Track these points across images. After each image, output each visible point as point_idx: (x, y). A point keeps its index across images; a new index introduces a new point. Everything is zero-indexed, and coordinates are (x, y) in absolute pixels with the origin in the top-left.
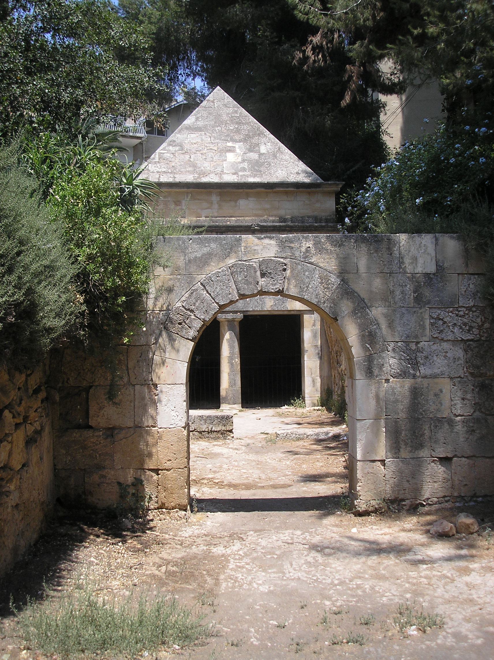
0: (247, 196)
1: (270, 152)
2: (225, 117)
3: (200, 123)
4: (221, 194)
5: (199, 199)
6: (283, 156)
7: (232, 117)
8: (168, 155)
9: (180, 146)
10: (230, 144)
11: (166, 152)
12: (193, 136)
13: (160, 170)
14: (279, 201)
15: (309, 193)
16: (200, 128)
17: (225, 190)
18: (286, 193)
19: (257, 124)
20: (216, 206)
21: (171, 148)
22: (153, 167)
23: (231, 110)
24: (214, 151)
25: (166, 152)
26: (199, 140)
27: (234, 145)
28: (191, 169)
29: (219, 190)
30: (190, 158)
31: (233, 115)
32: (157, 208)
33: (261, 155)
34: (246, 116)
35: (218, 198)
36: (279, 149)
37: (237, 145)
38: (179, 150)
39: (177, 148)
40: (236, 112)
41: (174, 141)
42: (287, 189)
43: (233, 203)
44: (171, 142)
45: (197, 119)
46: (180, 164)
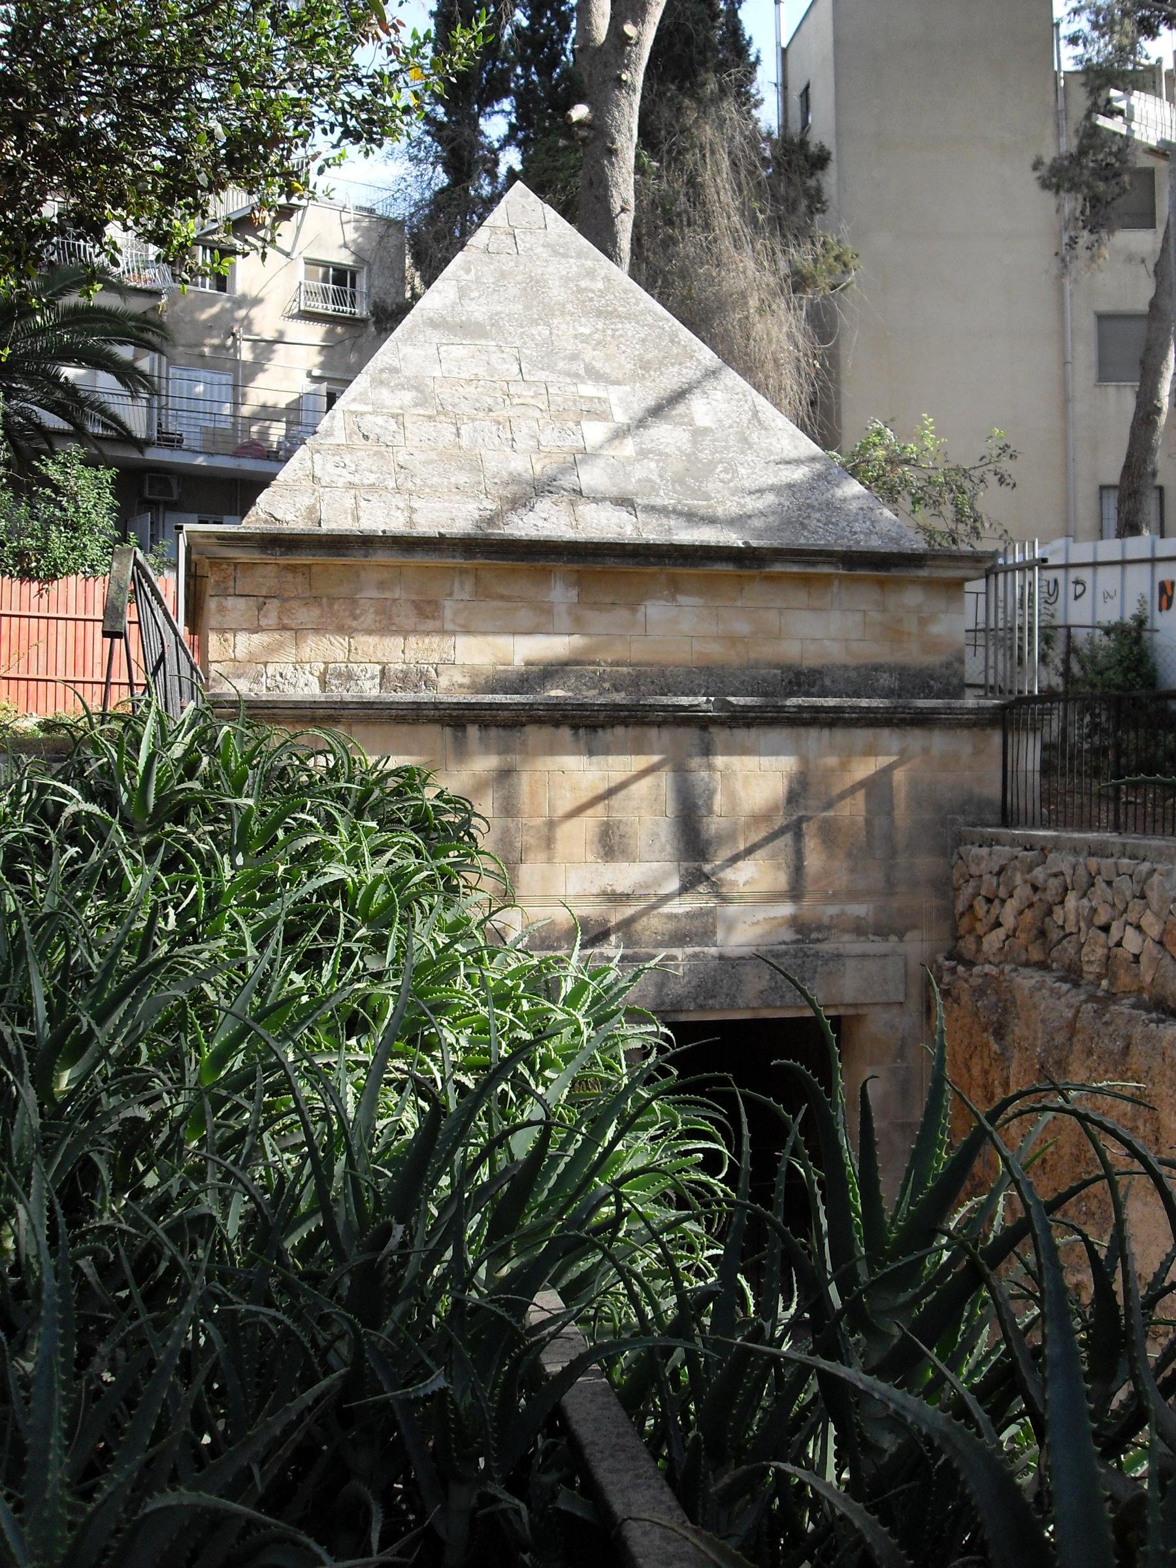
0: (675, 587)
1: (727, 423)
2: (557, 293)
3: (477, 310)
4: (580, 581)
5: (502, 597)
6: (774, 440)
7: (580, 290)
8: (380, 420)
9: (417, 389)
10: (588, 389)
11: (369, 408)
12: (458, 352)
13: (356, 479)
14: (781, 611)
15: (881, 584)
16: (477, 324)
17: (599, 568)
18: (806, 581)
19: (667, 320)
20: (564, 621)
21: (385, 394)
22: (330, 467)
23: (572, 266)
24: (538, 414)
25: (369, 408)
26: (482, 371)
27: (602, 395)
28: (462, 478)
29: (576, 567)
30: (458, 435)
31: (583, 284)
32: (354, 624)
33: (698, 434)
34: (626, 291)
35: (573, 594)
36: (755, 413)
37: (614, 395)
38: (416, 405)
39: (408, 397)
40: (591, 274)
41: (395, 370)
42: (810, 570)
43: (622, 614)
44: (382, 371)
45: (463, 292)
46: (422, 457)
